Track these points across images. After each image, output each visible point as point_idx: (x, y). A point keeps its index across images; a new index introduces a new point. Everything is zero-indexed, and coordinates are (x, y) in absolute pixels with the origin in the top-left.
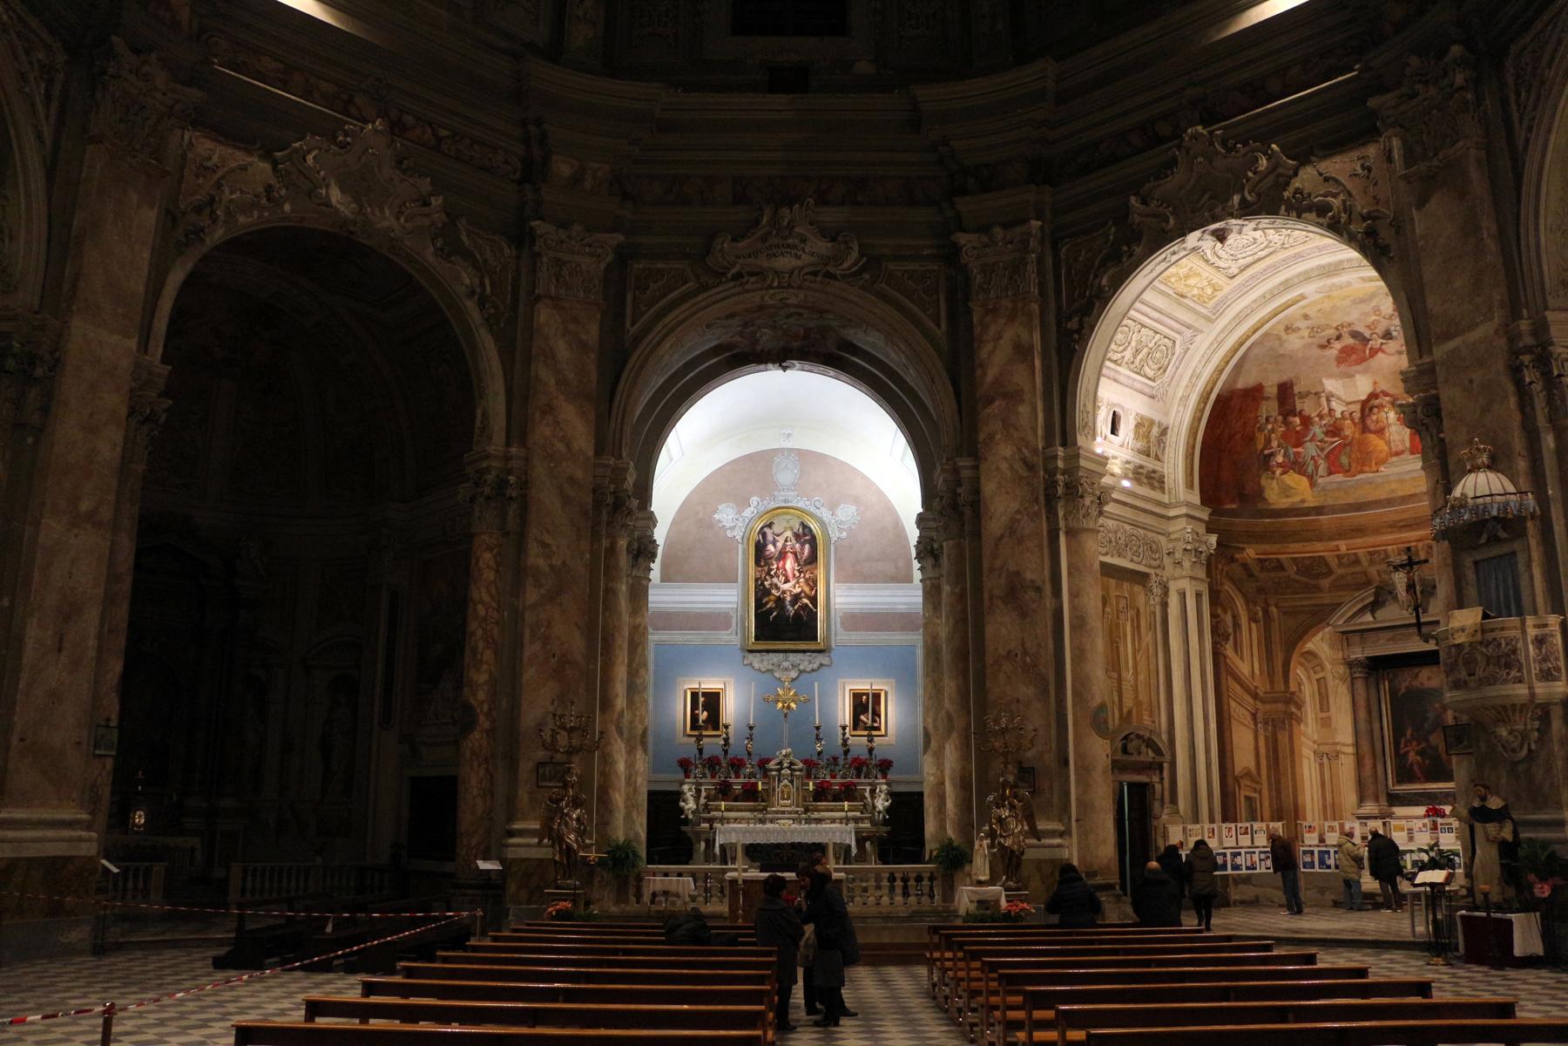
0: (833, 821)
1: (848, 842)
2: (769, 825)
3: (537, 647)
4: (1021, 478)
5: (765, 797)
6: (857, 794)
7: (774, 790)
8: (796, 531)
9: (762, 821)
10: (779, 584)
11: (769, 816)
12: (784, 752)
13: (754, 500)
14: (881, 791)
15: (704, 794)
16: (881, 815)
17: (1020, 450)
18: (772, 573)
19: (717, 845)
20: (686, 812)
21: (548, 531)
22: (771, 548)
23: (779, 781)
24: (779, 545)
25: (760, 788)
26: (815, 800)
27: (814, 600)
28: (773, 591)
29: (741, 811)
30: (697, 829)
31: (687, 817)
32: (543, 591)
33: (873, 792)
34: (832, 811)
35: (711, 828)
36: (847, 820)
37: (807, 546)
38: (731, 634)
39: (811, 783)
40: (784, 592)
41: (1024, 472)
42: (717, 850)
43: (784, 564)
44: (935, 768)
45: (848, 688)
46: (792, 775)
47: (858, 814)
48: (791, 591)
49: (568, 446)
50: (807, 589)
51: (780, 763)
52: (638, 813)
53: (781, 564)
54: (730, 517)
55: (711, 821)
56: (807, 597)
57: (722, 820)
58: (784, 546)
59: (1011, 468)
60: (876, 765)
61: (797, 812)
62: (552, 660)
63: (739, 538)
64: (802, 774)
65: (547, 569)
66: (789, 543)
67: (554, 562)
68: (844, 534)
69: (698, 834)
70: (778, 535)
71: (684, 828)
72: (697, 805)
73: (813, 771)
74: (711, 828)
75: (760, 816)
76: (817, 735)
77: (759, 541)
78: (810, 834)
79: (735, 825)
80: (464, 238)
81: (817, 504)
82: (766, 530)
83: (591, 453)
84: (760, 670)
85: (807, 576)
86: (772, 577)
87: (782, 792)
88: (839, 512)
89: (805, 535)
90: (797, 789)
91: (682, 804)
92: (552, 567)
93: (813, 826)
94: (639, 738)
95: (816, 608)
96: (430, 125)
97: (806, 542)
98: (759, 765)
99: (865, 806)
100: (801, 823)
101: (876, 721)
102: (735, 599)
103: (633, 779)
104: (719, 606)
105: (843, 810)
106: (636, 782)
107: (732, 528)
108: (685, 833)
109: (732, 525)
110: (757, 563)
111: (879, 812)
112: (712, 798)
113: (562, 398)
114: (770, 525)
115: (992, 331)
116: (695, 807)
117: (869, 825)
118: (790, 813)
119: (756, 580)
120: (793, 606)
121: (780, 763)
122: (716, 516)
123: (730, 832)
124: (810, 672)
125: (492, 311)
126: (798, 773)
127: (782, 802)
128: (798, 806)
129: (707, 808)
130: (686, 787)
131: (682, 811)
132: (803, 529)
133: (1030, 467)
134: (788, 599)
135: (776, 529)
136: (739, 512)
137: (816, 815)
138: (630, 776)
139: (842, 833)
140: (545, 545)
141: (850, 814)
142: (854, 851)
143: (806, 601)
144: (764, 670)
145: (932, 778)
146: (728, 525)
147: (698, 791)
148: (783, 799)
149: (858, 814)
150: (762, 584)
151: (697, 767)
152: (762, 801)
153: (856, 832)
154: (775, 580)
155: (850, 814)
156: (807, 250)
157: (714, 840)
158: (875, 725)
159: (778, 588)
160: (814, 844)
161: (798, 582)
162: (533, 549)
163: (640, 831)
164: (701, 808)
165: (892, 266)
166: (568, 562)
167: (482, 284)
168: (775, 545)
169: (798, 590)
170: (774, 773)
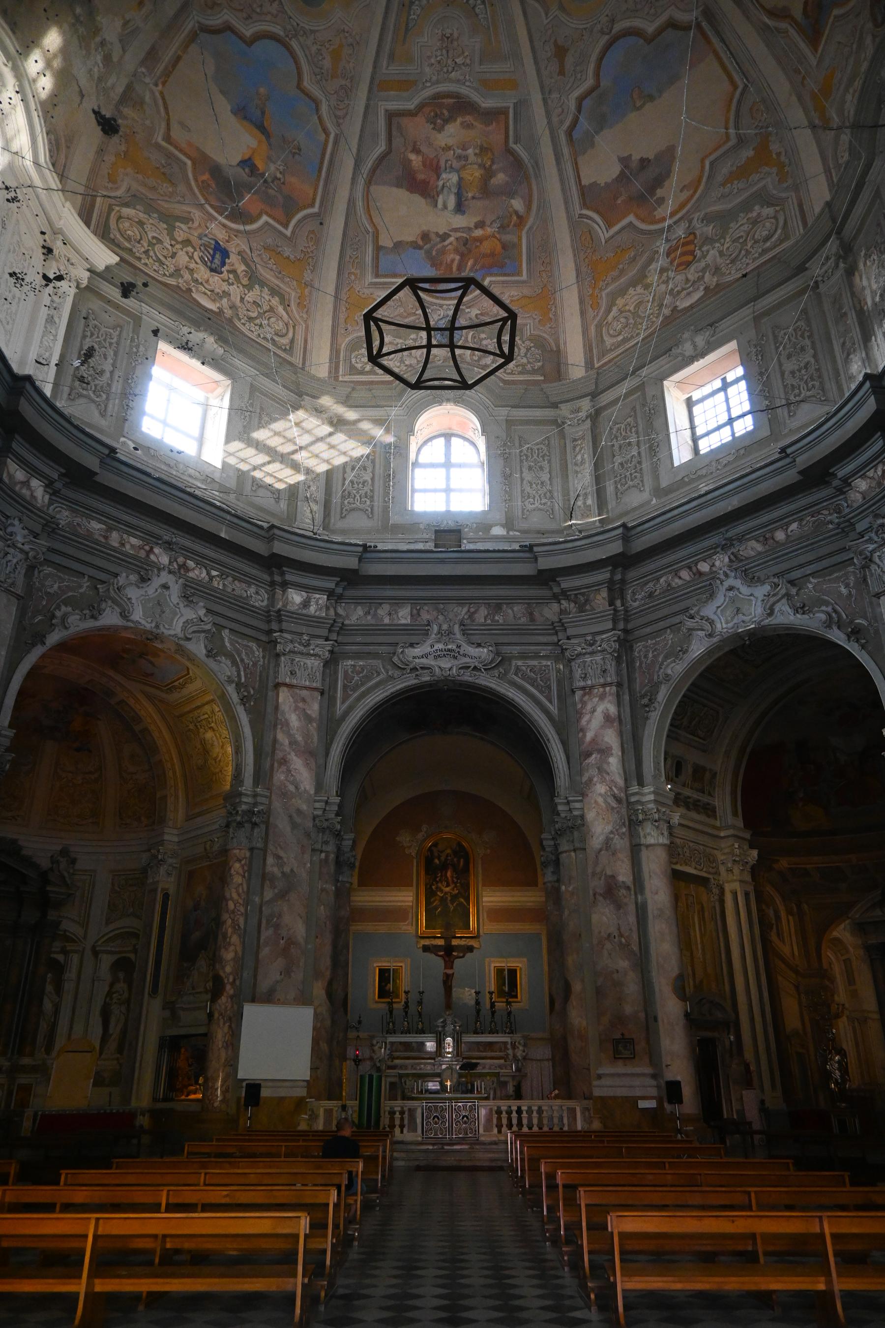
3: (271, 931)
4: (613, 808)
13: (424, 828)
17: (610, 788)
21: (281, 848)
22: (437, 861)
32: (276, 891)
38: (408, 925)
40: (446, 893)
41: (614, 804)
43: (446, 873)
45: (493, 965)
49: (297, 788)
58: (446, 860)
59: (606, 801)
62: (282, 942)
63: (413, 854)
65: (280, 875)
67: (285, 870)
80: (227, 644)
83: (312, 792)
86: (437, 882)
92: (283, 873)
96: (206, 569)
99: (507, 1055)
104: (399, 904)
113: (293, 754)
115: (589, 707)
125: (246, 694)
133: (618, 800)
140: (279, 857)
156: (461, 653)
159: (442, 891)
162: (270, 860)
165: (520, 663)
166: (295, 870)
167: (239, 675)
168: (439, 859)
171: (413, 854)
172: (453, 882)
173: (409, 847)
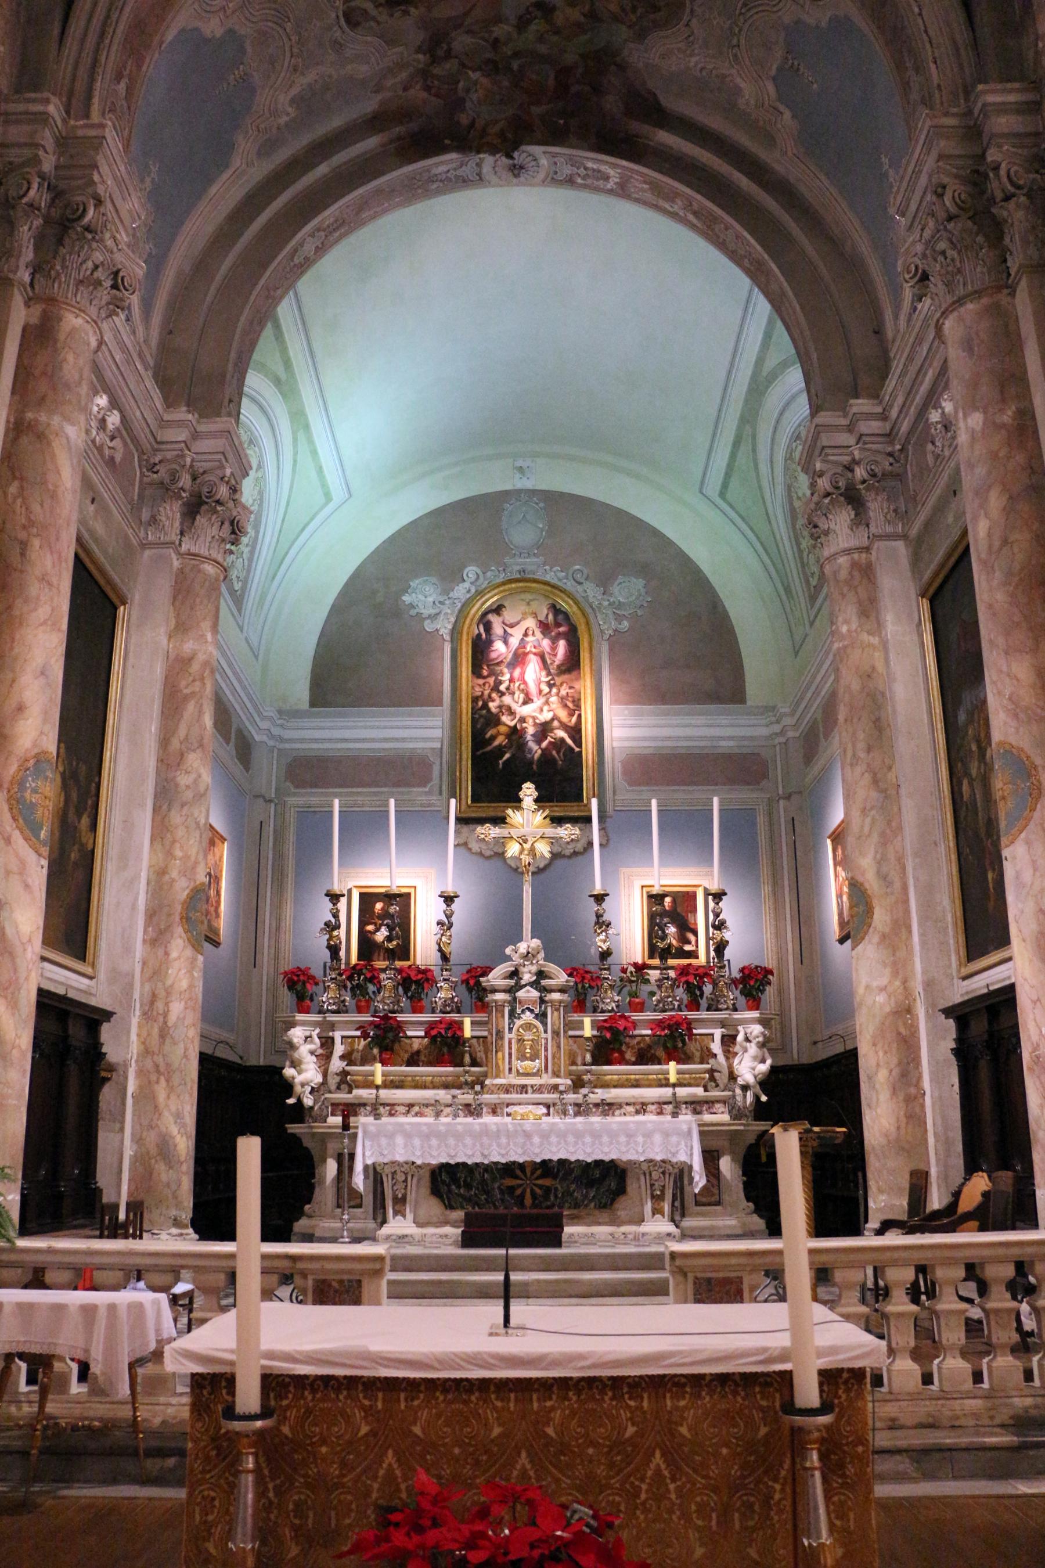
0: (642, 1108)
1: (682, 1157)
2: (488, 1119)
5: (480, 1055)
6: (692, 1047)
7: (500, 1035)
8: (542, 618)
9: (472, 1110)
10: (515, 707)
11: (487, 1097)
12: (523, 947)
13: (471, 572)
14: (747, 1040)
15: (339, 1049)
16: (749, 1095)
18: (502, 688)
19: (359, 1167)
20: (298, 1089)
22: (499, 646)
23: (512, 1014)
24: (514, 642)
25: (468, 1033)
26: (596, 1062)
27: (576, 732)
28: (505, 719)
29: (424, 1086)
30: (319, 1128)
31: (299, 1101)
33: (729, 1040)
34: (636, 1085)
35: (346, 1126)
36: (676, 1105)
37: (562, 644)
38: (430, 793)
39: (587, 1021)
40: (523, 720)
42: (359, 1181)
43: (523, 674)
44: (887, 971)
46: (542, 1001)
47: (699, 1091)
48: (534, 718)
50: (563, 714)
51: (515, 974)
52: (171, 1089)
53: (517, 673)
54: (431, 599)
55: (349, 1110)
56: (564, 726)
57: (376, 1108)
58: (523, 643)
60: (735, 982)
61: (555, 1088)
64: (565, 997)
66: (530, 639)
68: (626, 624)
69: (323, 1139)
70: (512, 626)
71: (293, 1128)
72: (325, 1075)
73: (591, 998)
74: (346, 1126)
75: (468, 1097)
76: (599, 916)
77: (479, 635)
78: (588, 1139)
79: (410, 1119)
81: (578, 576)
82: (492, 617)
84: (481, 854)
85: (563, 692)
86: (503, 694)
87: (521, 1040)
88: (615, 589)
89: (558, 625)
90: (556, 1033)
91: (289, 1072)
93: (596, 1120)
94: (178, 908)
95: (580, 745)
97: (559, 636)
98: (466, 982)
100: (565, 1113)
101: (689, 943)
102: (438, 733)
103: (160, 1005)
105: (666, 1084)
106: (166, 1015)
107: (433, 617)
108: (296, 1139)
109: (433, 611)
110: (476, 671)
111: (745, 1088)
112: (357, 1056)
114: (498, 610)
116: (319, 1079)
117: (726, 1118)
118: (539, 1089)
119: (475, 700)
120: (539, 742)
121: (515, 974)
122: (407, 598)
123: (391, 1136)
124: (570, 857)
126: (556, 996)
127: (518, 1064)
128: (556, 1074)
129: (345, 1081)
130: (297, 1034)
131: (288, 1087)
132: (555, 615)
134: (531, 730)
135: (509, 615)
136: (446, 592)
137: (601, 1094)
138: (154, 996)
139: (667, 1135)
141: (682, 1092)
142: (699, 1180)
143: (561, 734)
144: (488, 853)
145: (881, 998)
146: (426, 612)
147: (327, 1043)
148: (522, 1057)
149: (699, 1091)
150: (485, 706)
151: (326, 989)
152: (474, 1063)
153: (702, 1134)
154: (507, 700)
155: (682, 1092)
157: (352, 1156)
158: (687, 948)
159: (511, 712)
160: (598, 1163)
161: (547, 703)
163: (174, 1130)
164: (333, 1081)
168: (506, 642)
169: (547, 716)
170: (500, 996)
171: (443, 631)
172: (540, 691)
173: (433, 617)
